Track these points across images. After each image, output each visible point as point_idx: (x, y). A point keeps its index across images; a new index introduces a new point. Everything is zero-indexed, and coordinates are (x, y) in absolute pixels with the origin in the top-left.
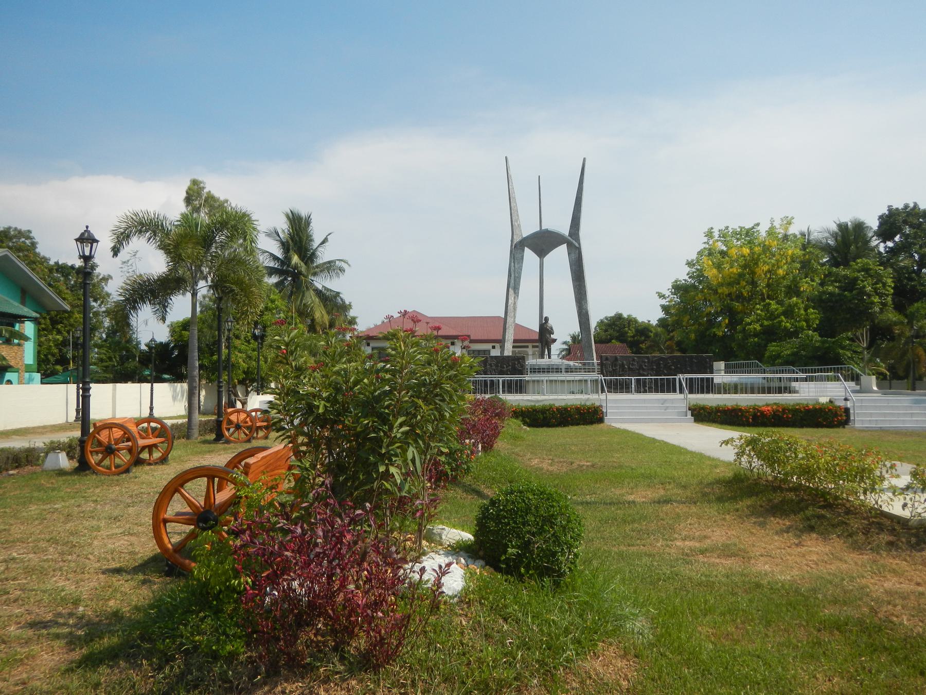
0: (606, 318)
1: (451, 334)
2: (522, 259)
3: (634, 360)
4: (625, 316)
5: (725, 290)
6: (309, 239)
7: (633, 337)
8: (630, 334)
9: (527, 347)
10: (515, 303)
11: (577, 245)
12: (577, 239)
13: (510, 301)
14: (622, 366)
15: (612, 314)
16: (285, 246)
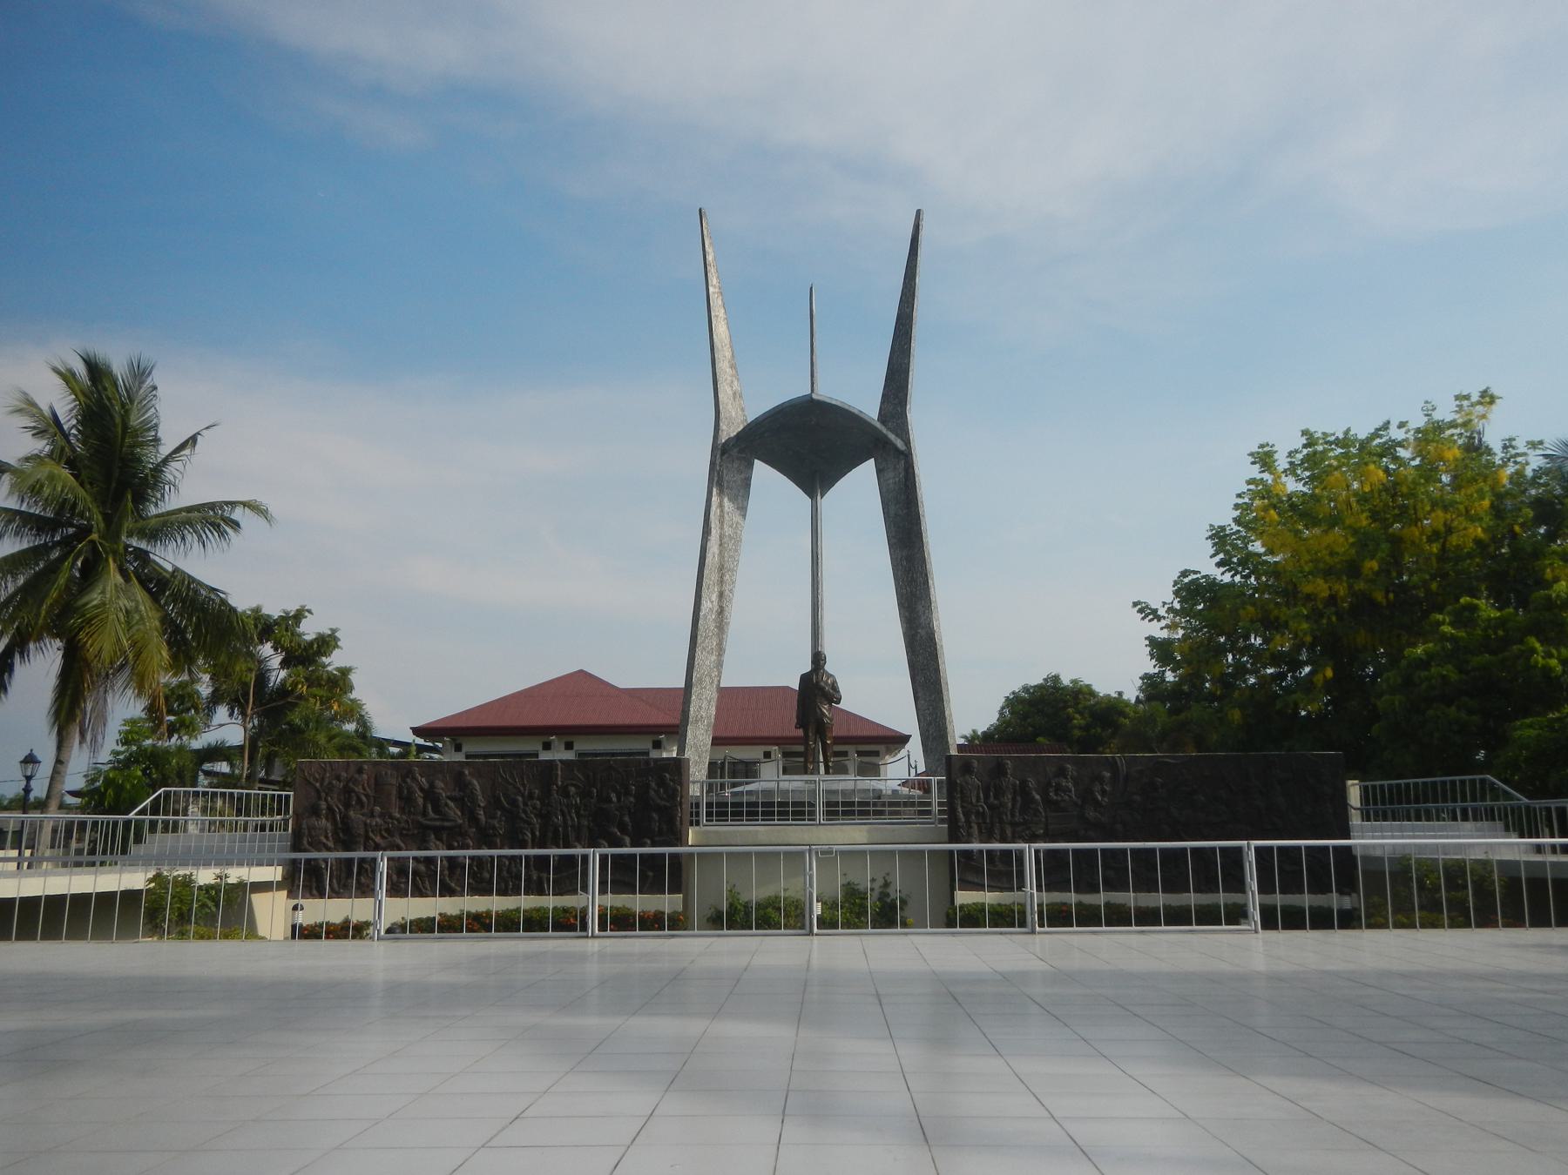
0: (1026, 689)
1: (652, 721)
2: (747, 484)
3: (1062, 772)
4: (1066, 681)
5: (1321, 587)
6: (146, 435)
7: (1086, 728)
8: (1078, 720)
9: (845, 754)
10: (721, 611)
11: (899, 444)
12: (903, 430)
13: (706, 605)
14: (1023, 790)
15: (1036, 679)
16: (63, 455)
